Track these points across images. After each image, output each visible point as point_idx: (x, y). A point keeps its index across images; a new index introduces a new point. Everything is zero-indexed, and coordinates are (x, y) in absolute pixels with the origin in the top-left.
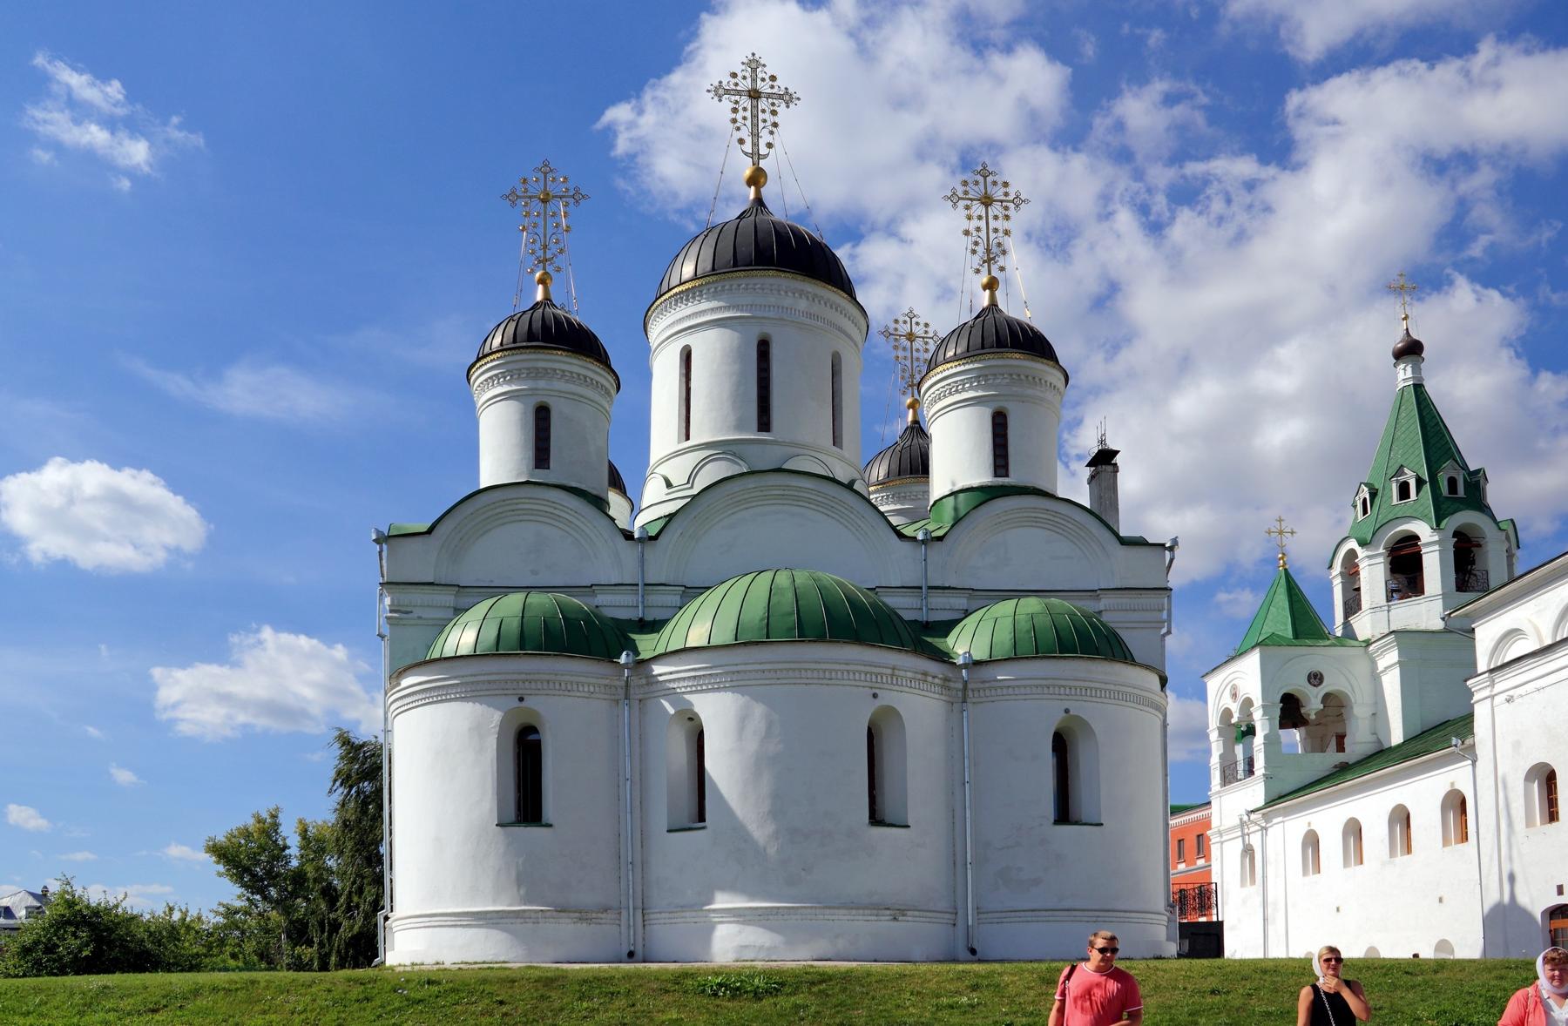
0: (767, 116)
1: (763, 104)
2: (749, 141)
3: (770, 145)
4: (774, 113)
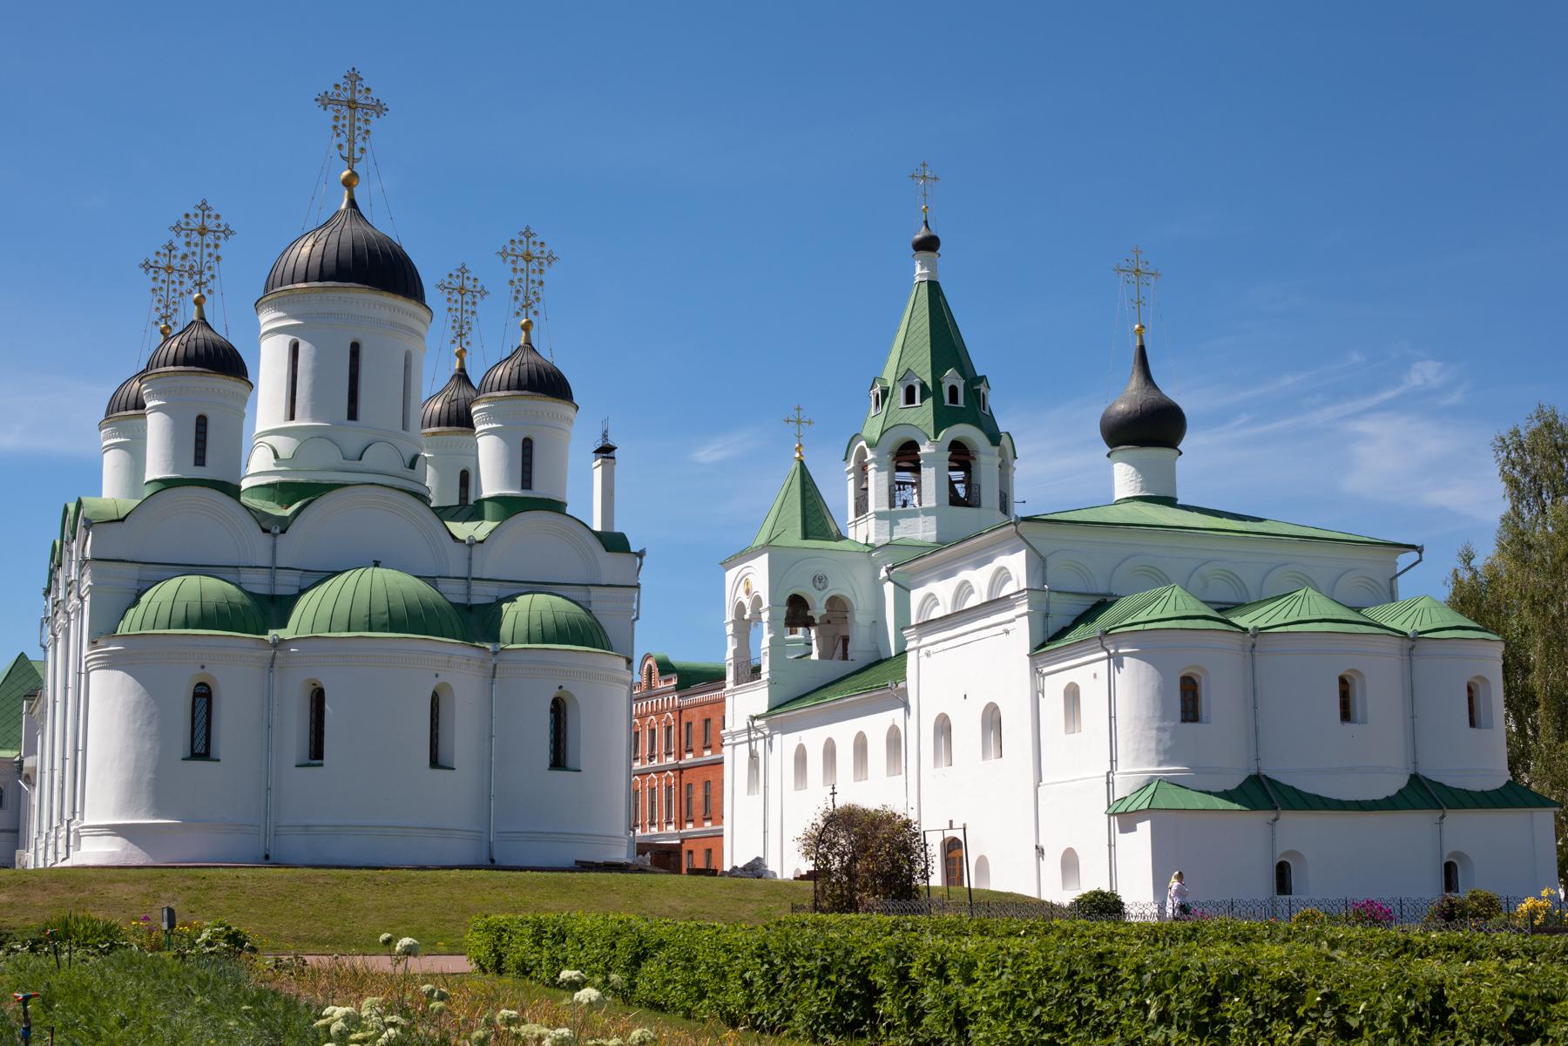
0: (361, 124)
1: (359, 114)
2: (346, 146)
3: (362, 150)
4: (367, 121)
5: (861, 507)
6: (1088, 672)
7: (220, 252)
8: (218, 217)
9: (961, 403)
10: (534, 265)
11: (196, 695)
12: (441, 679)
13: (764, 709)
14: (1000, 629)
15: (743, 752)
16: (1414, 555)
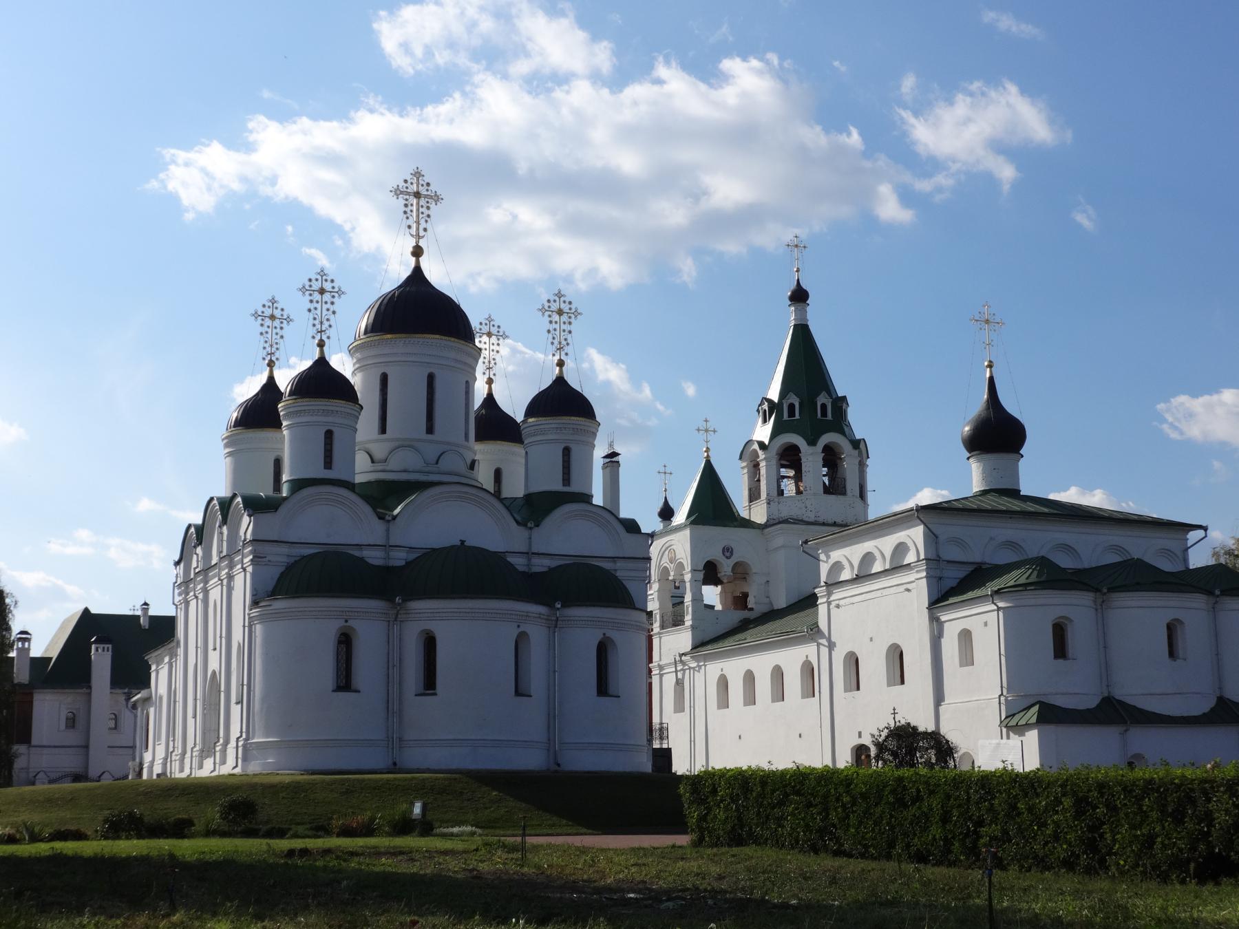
1: (423, 201)
2: (414, 226)
3: (425, 230)
4: (428, 208)
5: (754, 496)
6: (982, 622)
7: (572, 328)
8: (332, 281)
9: (830, 416)
10: (564, 318)
11: (340, 642)
12: (521, 629)
13: (688, 647)
14: (902, 588)
15: (670, 681)
16: (1201, 533)
